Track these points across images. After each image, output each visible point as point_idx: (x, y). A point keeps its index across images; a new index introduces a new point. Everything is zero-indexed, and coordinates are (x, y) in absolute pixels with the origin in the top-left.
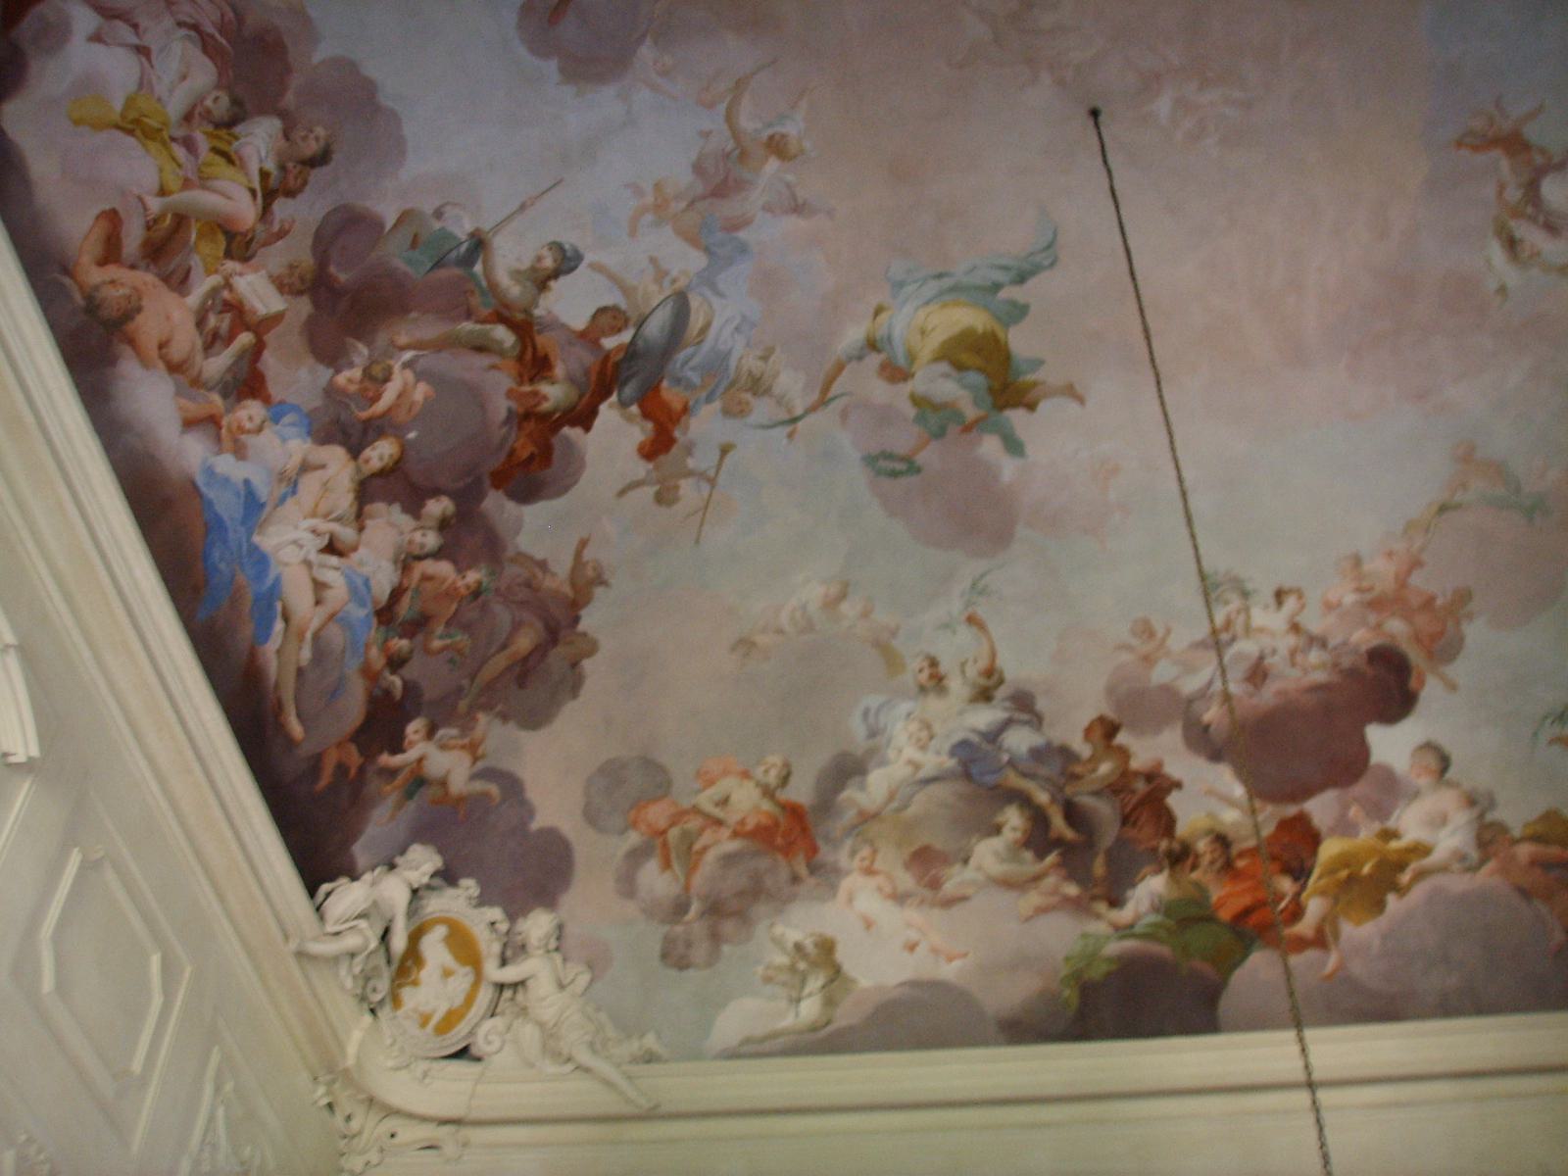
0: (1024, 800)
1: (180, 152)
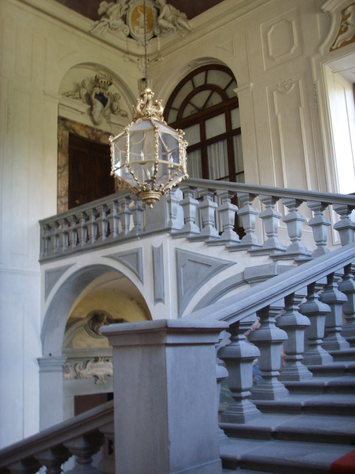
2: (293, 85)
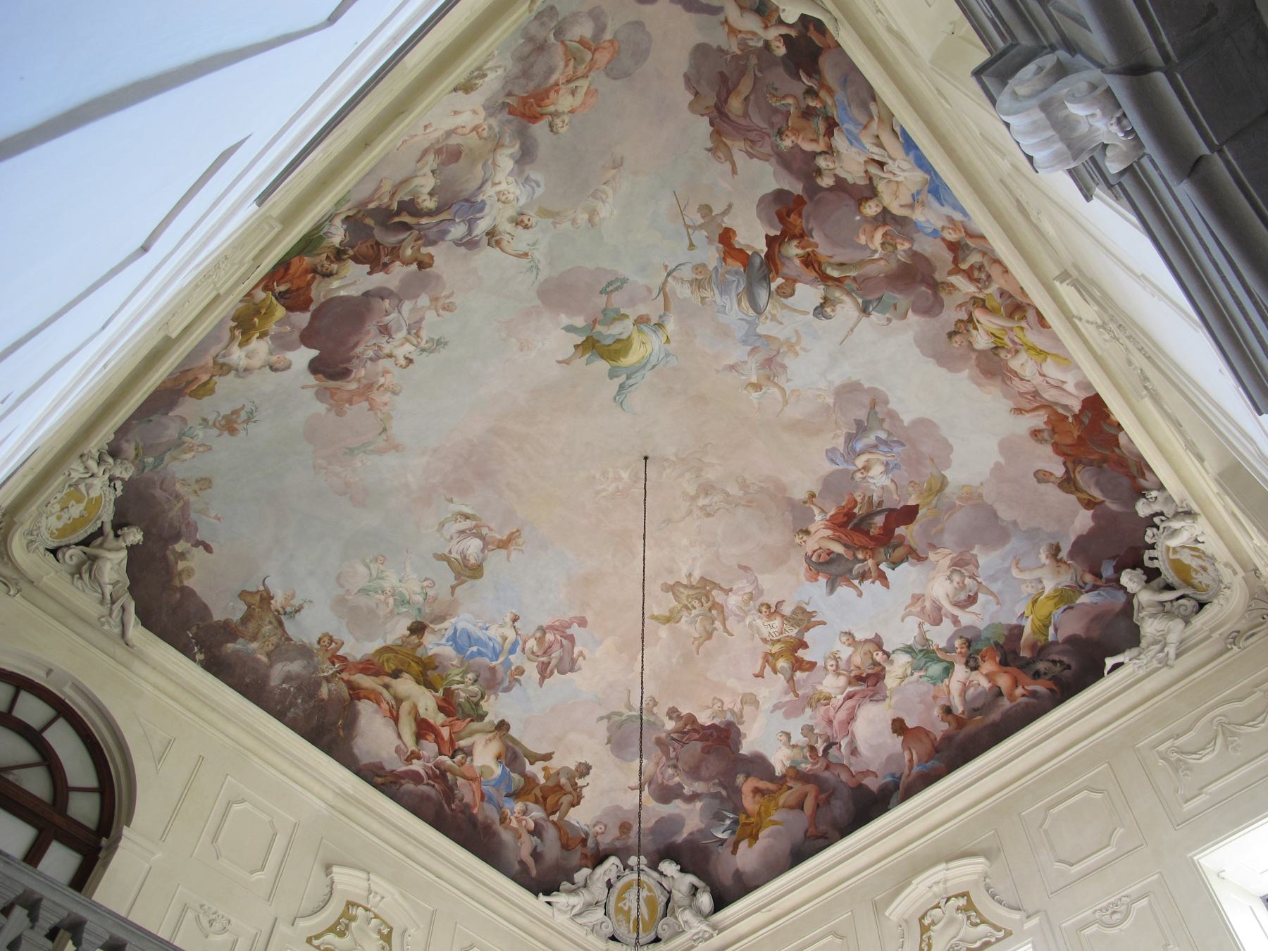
0: (430, 213)
1: (1016, 340)
2: (225, 936)
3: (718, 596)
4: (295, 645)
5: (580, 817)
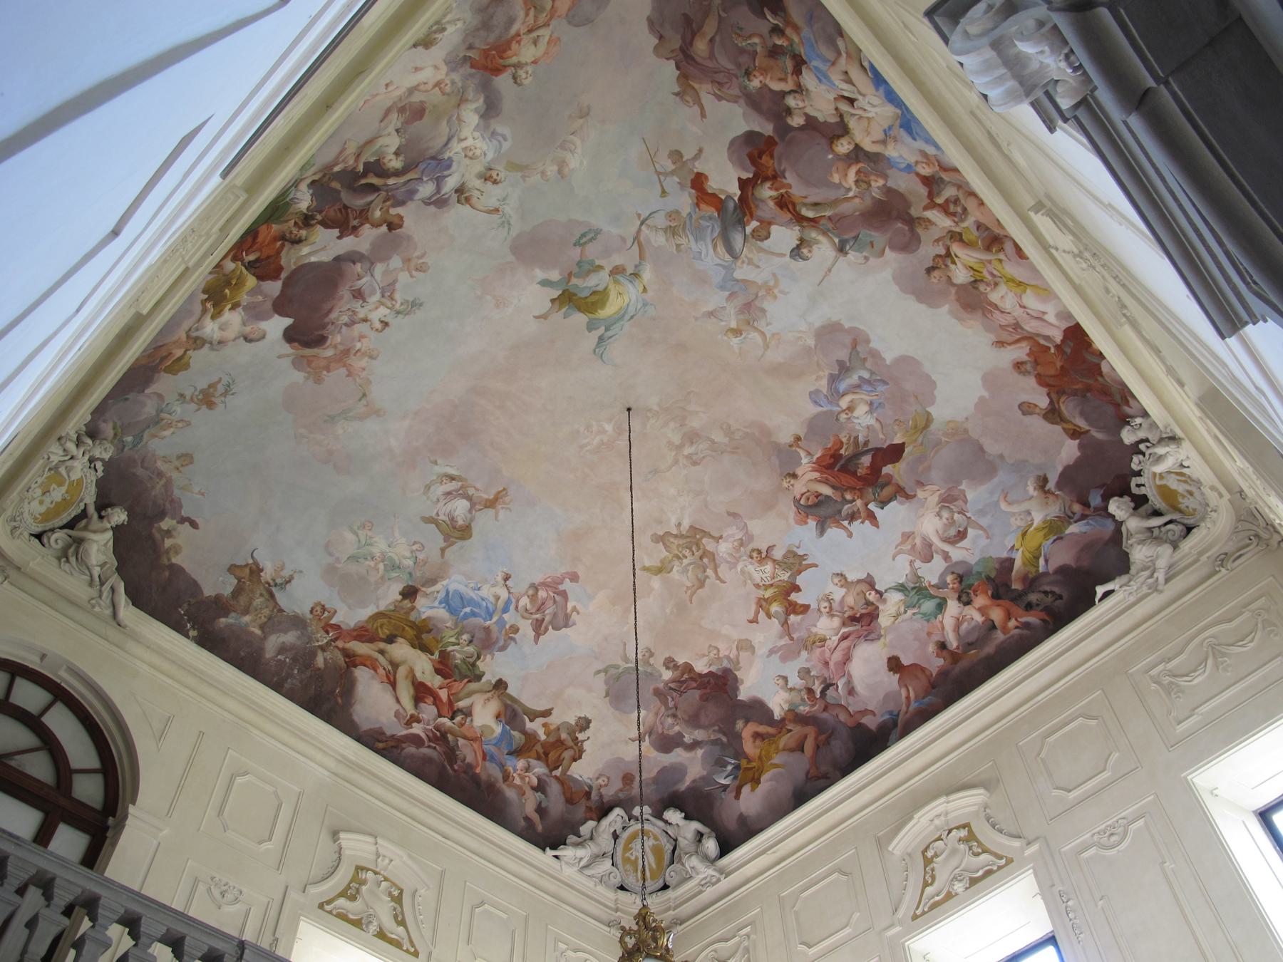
0: (397, 173)
1: (995, 272)
3: (708, 544)
4: (288, 616)
5: (583, 771)
